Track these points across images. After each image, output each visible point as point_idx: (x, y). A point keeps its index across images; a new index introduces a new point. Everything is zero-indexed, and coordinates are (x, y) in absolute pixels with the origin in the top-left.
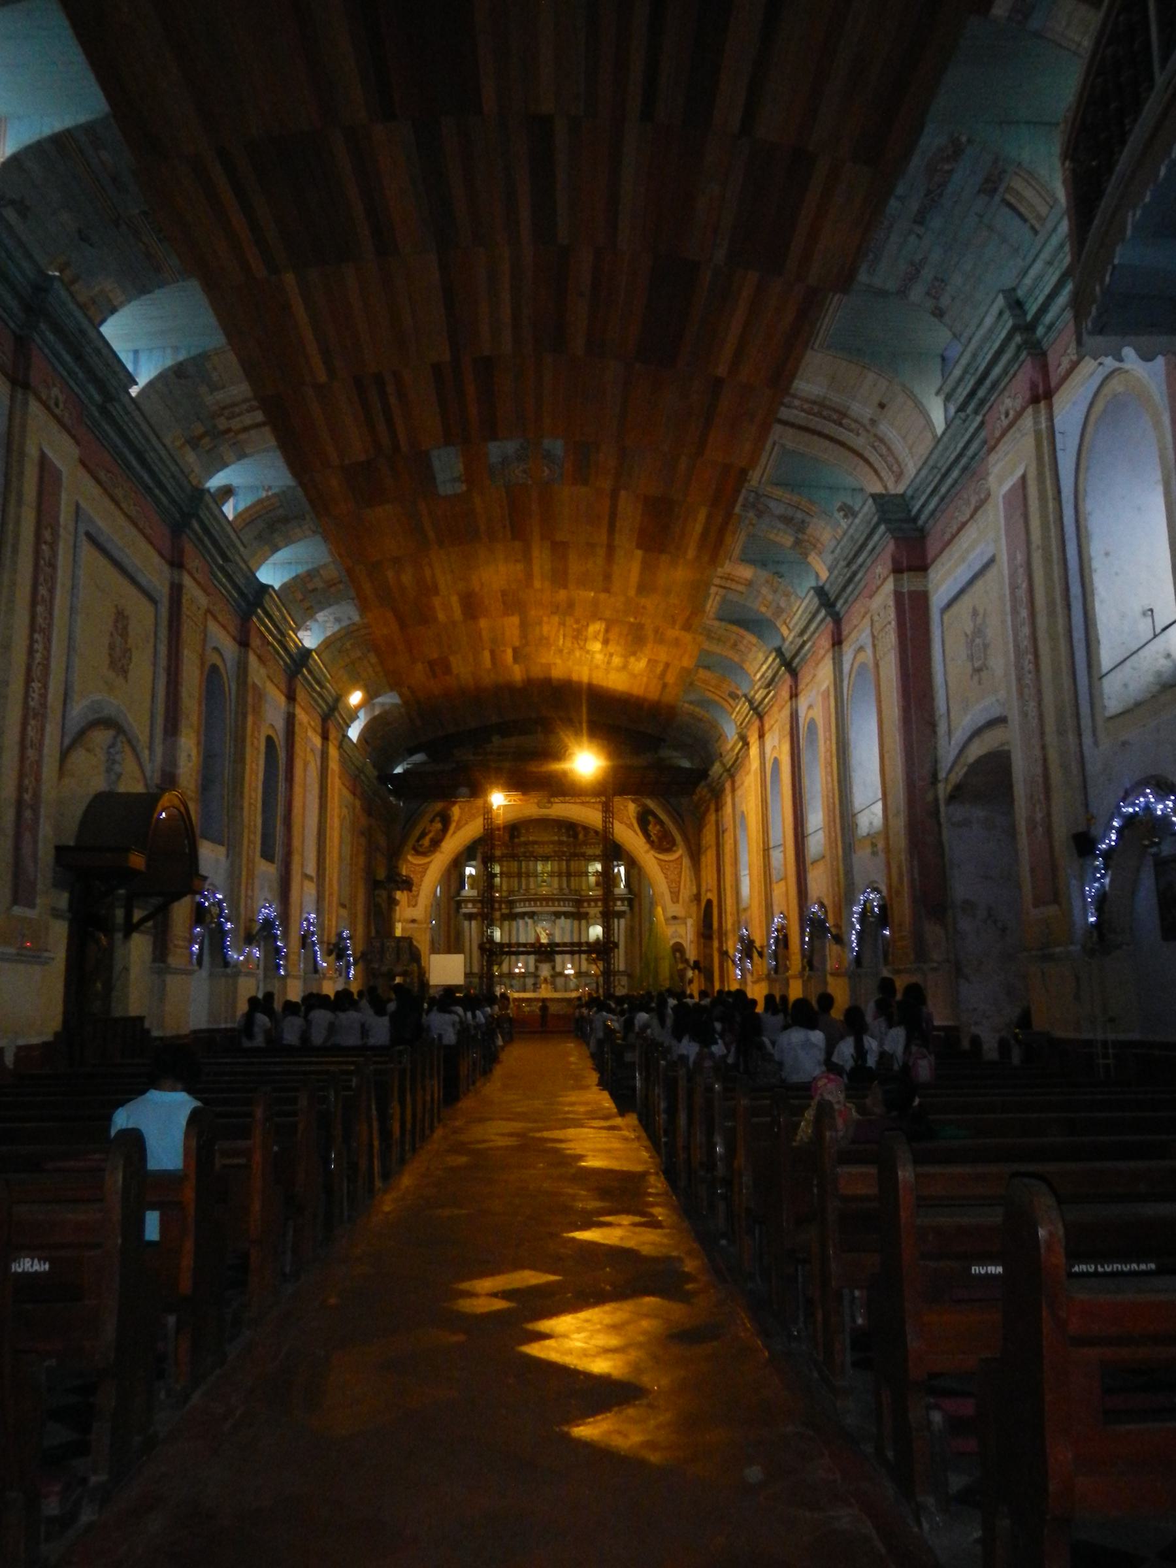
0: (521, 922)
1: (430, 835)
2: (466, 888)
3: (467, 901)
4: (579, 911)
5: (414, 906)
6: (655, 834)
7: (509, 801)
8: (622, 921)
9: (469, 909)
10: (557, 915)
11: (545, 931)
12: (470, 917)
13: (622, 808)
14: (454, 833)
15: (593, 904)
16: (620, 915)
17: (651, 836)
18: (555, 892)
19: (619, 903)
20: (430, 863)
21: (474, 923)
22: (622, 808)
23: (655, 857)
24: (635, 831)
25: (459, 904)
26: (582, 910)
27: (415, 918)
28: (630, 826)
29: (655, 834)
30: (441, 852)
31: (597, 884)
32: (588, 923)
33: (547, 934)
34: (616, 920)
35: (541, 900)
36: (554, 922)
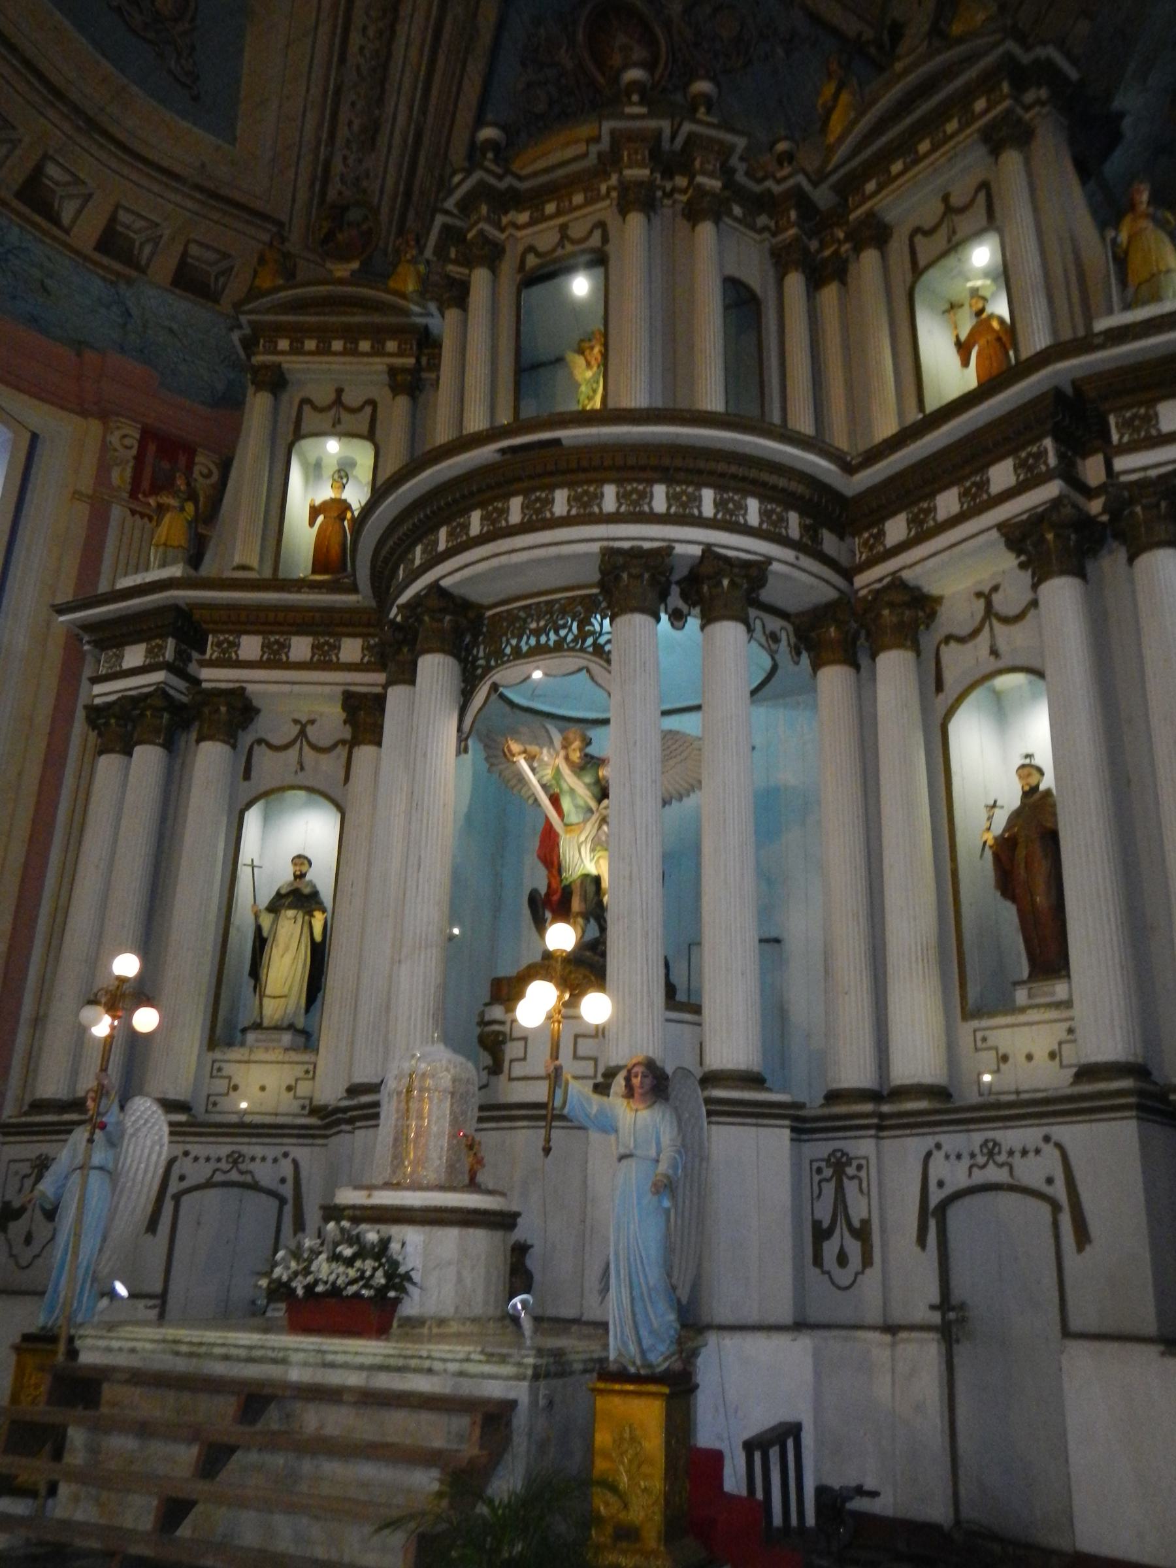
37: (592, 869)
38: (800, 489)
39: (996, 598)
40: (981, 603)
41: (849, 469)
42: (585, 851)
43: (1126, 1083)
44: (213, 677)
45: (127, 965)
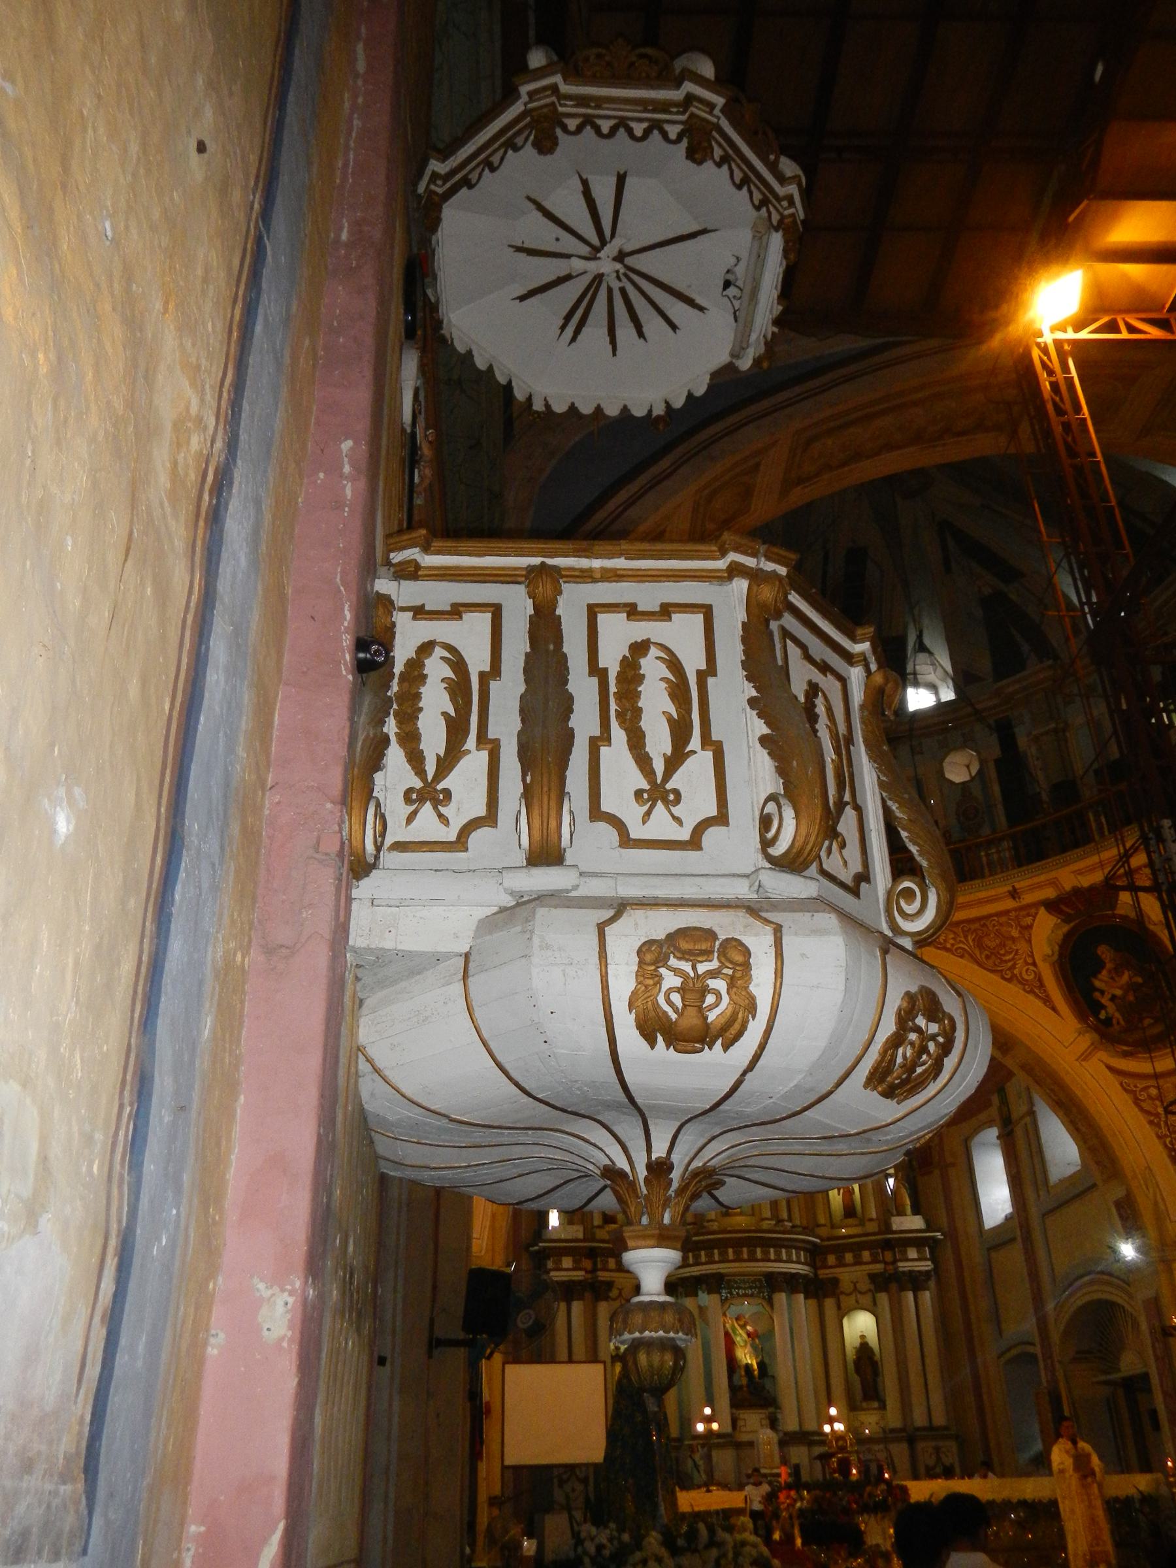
3: (560, 1249)
4: (816, 1275)
6: (1113, 998)
7: (1112, 327)
8: (926, 1296)
9: (565, 1271)
10: (772, 1284)
11: (743, 1327)
13: (1015, 933)
15: (849, 1257)
16: (916, 1282)
17: (1097, 1007)
18: (766, 1225)
19: (912, 1253)
21: (577, 1306)
22: (1015, 933)
23: (1110, 1068)
24: (1047, 1001)
25: (540, 1257)
26: (823, 1273)
28: (1036, 987)
29: (1113, 998)
31: (850, 1211)
32: (839, 1308)
33: (749, 1335)
34: (910, 1295)
35: (738, 1244)
36: (770, 1302)
37: (749, 1362)
38: (808, 1246)
39: (858, 1285)
40: (852, 1285)
41: (822, 1240)
42: (748, 1356)
43: (904, 1434)
44: (603, 1276)
45: (708, 1411)
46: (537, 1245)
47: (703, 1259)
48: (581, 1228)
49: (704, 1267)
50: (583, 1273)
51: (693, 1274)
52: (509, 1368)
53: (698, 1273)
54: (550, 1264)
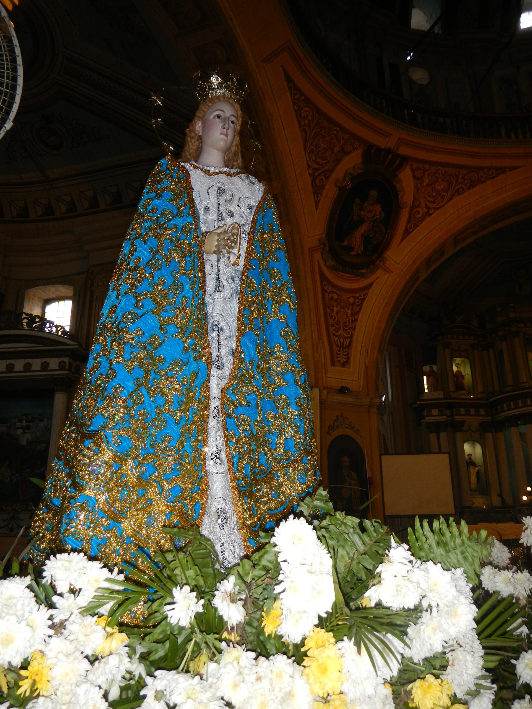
0: (513, 432)
1: (363, 229)
2: (426, 391)
5: (343, 365)
12: (437, 427)
14: (407, 233)
20: (369, 287)
21: (443, 435)
27: (344, 385)
30: (388, 271)
44: (457, 418)
46: (416, 404)
47: (520, 405)
48: (442, 393)
49: (521, 409)
50: (445, 417)
51: (515, 414)
52: (383, 457)
53: (518, 413)
54: (425, 414)
